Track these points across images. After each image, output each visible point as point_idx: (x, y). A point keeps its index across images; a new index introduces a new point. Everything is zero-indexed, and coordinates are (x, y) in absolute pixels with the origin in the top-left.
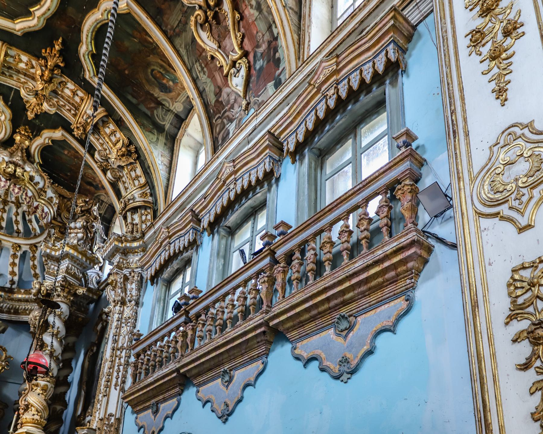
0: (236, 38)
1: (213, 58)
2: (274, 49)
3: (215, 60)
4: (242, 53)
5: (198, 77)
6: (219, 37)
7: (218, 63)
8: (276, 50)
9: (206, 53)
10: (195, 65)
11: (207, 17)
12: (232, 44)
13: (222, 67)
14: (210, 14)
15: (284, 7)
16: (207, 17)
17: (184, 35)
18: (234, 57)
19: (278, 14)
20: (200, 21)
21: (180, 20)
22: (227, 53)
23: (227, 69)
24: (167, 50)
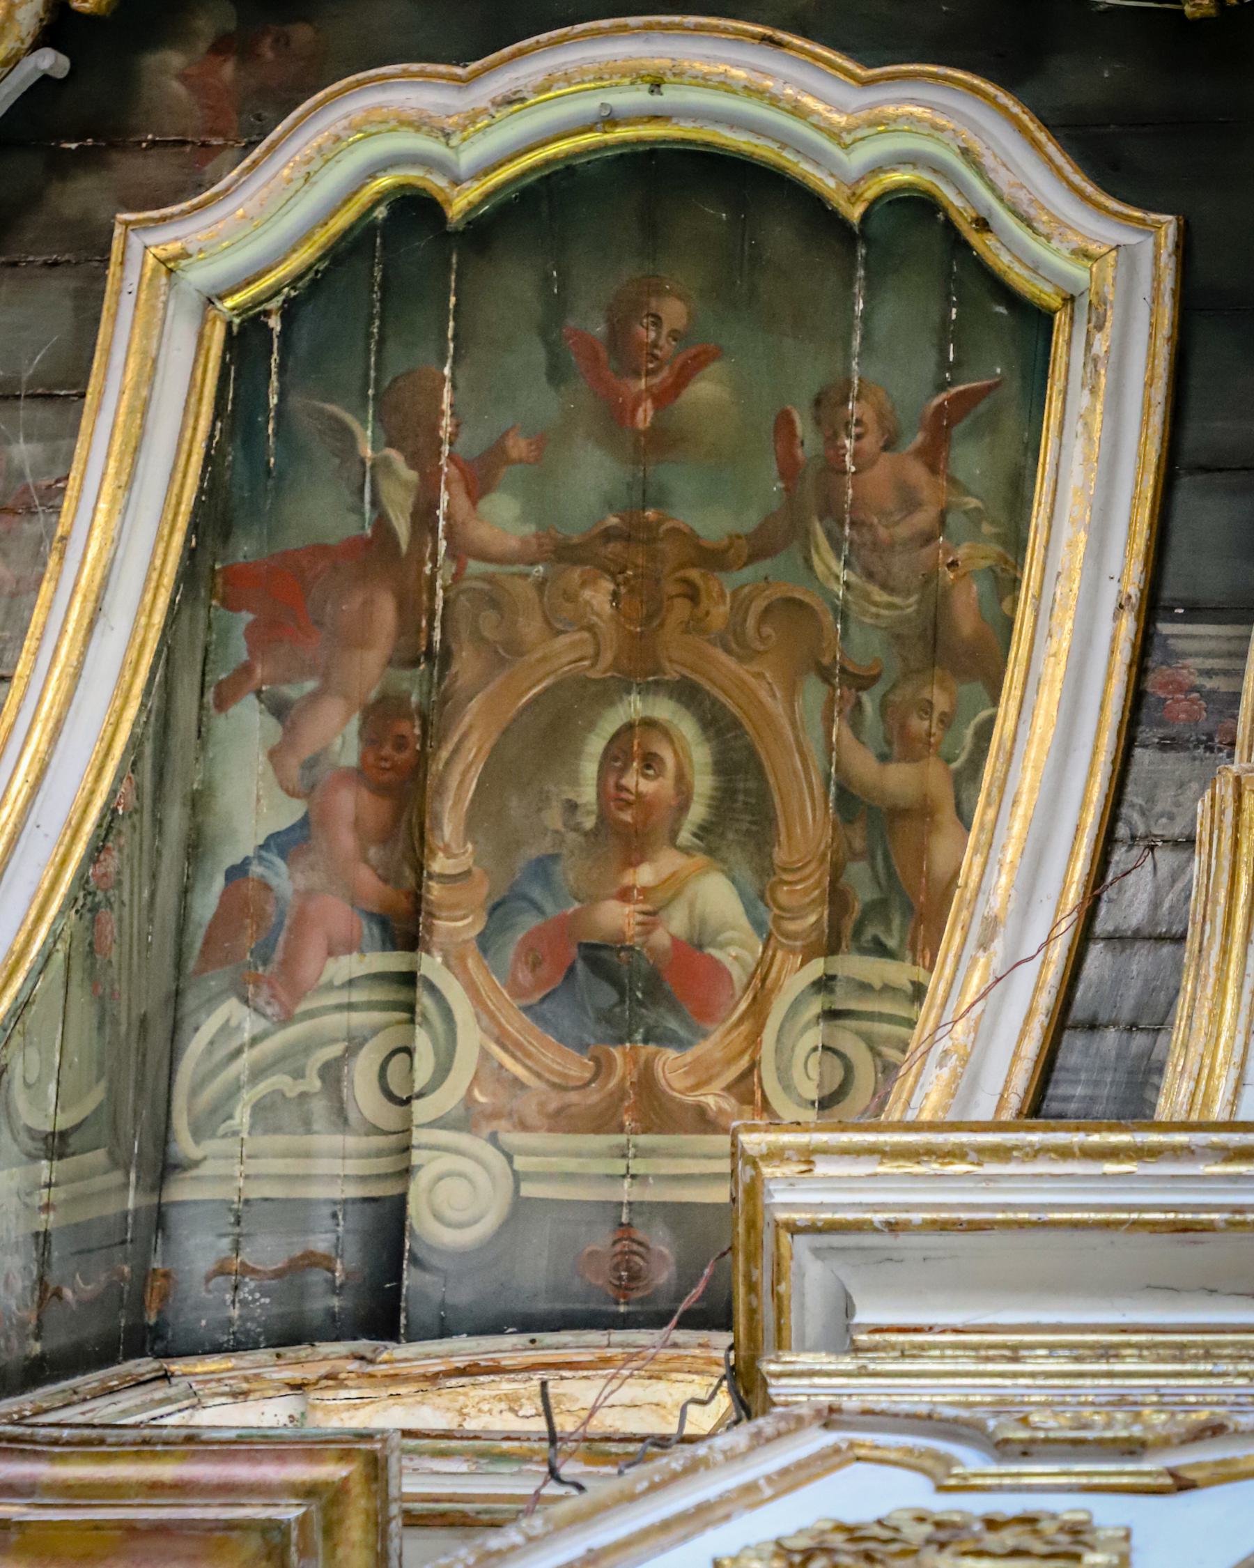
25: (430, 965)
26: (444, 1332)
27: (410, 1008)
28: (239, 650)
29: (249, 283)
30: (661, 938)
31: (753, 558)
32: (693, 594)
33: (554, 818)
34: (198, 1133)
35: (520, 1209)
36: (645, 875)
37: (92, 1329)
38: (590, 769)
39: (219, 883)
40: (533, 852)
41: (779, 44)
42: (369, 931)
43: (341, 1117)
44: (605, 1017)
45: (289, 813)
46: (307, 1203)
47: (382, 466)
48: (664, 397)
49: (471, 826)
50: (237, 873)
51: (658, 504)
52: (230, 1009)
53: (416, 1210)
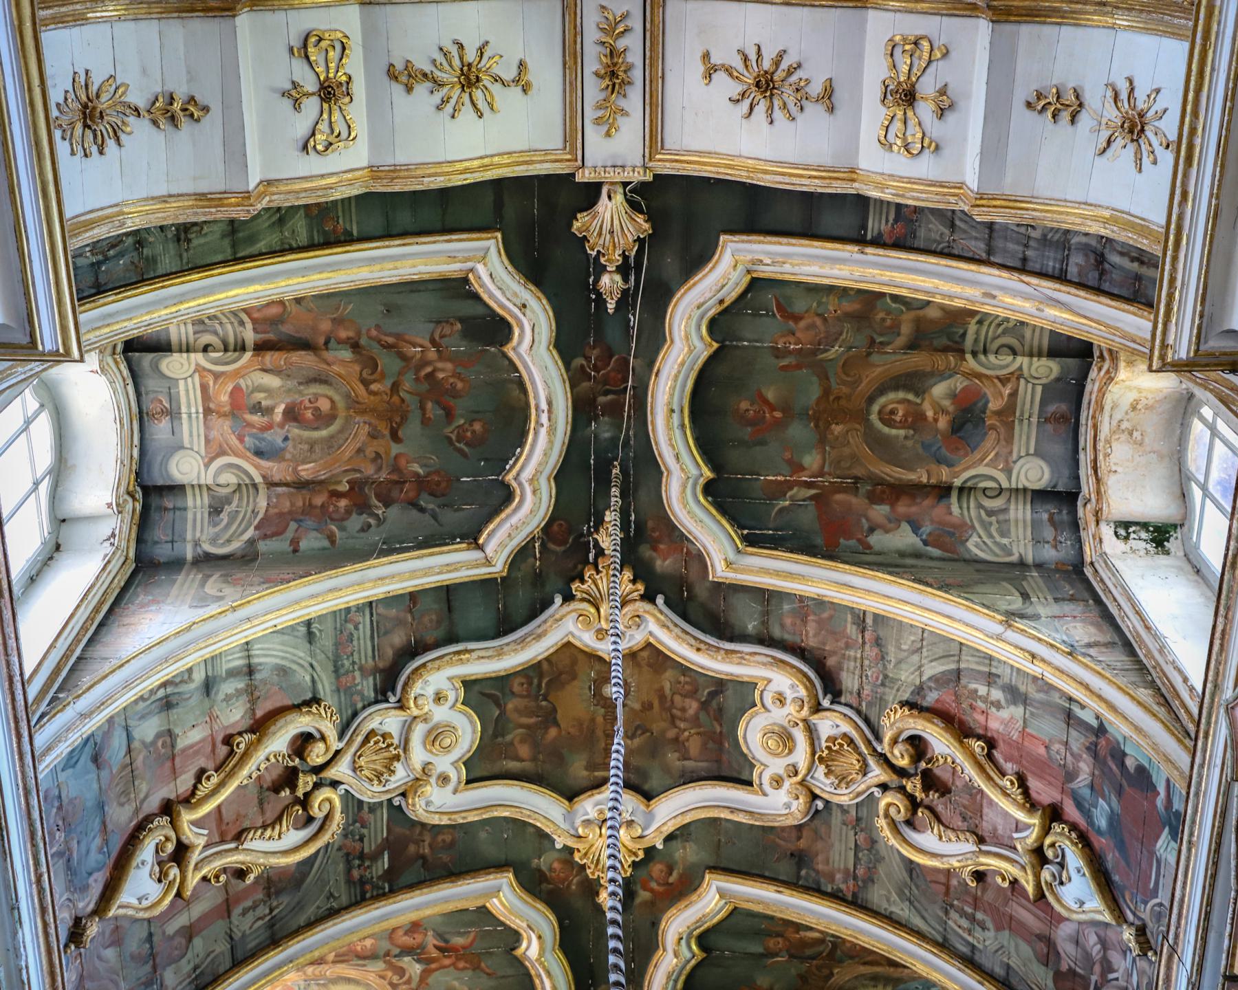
0: (1006, 795)
1: (979, 876)
2: (1113, 756)
3: (989, 879)
4: (1043, 817)
5: (973, 946)
6: (964, 819)
7: (999, 880)
8: (1119, 756)
9: (957, 876)
11: (911, 798)
12: (1006, 814)
13: (1014, 882)
14: (914, 786)
15: (1070, 654)
16: (911, 798)
17: (881, 870)
18: (1030, 841)
19: (1064, 677)
20: (900, 818)
22: (1006, 841)
23: (1031, 878)
24: (862, 931)
25: (958, 482)
26: (1077, 478)
27: (970, 489)
28: (852, 542)
30: (951, 409)
31: (828, 379)
32: (838, 398)
33: (909, 443)
34: (1011, 554)
35: (1037, 454)
36: (930, 414)
37: (1080, 586)
38: (894, 432)
39: (929, 548)
40: (920, 451)
41: (658, 371)
42: (944, 503)
43: (1005, 510)
44: (976, 426)
45: (905, 527)
46: (1033, 521)
47: (792, 498)
48: (773, 408)
49: (911, 469)
50: (926, 543)
51: (807, 410)
52: (970, 545)
53: (1037, 486)
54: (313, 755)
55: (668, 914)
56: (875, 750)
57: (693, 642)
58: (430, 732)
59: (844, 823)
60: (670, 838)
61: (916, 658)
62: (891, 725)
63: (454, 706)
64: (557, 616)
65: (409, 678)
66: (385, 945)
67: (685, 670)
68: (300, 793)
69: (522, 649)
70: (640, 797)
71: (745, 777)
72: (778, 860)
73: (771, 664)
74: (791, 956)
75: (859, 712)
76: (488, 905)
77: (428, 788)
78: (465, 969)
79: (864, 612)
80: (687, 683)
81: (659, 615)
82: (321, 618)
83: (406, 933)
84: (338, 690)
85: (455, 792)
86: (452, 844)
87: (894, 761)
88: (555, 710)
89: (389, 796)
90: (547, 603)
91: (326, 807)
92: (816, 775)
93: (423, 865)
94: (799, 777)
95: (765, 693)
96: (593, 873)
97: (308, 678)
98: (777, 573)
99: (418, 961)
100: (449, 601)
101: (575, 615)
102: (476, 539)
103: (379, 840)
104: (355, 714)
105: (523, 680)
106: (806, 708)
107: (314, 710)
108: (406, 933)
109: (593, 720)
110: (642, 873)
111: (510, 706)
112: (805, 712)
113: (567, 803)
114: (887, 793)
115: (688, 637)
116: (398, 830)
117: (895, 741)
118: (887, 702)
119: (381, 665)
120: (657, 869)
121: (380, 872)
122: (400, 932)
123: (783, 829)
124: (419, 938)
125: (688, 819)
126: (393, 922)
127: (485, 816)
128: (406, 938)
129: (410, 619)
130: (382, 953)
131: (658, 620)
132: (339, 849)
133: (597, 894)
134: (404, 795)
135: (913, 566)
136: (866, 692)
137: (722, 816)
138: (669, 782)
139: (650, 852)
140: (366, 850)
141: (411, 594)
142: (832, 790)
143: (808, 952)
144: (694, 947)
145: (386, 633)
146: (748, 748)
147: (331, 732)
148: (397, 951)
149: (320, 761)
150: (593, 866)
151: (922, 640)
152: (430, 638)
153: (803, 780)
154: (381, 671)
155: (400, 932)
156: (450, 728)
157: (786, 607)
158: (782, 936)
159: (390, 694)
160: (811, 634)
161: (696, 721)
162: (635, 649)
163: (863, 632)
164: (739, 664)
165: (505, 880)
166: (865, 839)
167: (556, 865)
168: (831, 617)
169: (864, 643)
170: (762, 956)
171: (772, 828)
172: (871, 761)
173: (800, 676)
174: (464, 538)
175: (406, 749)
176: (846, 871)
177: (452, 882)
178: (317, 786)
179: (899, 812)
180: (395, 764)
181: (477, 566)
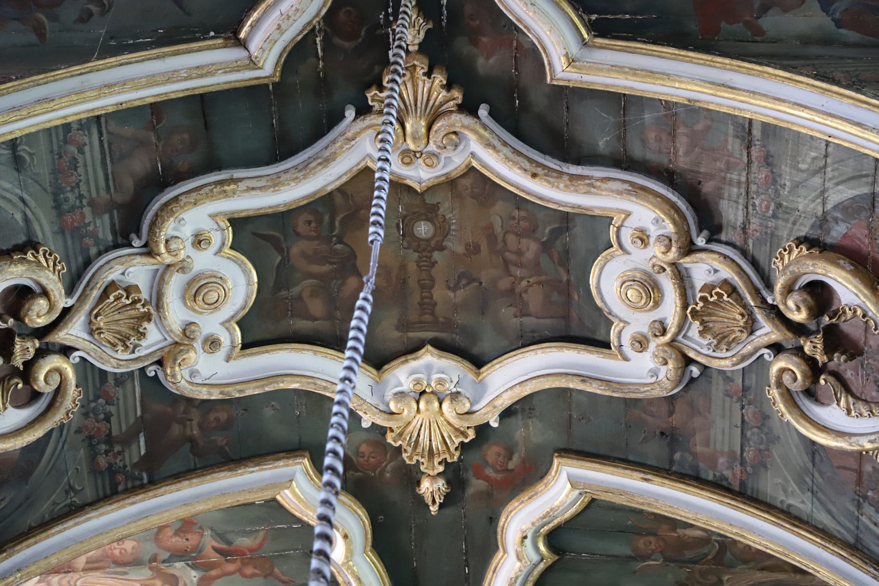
10: (864, 519)
16: (810, 362)
17: (776, 452)
21: (743, 421)
24: (752, 530)
29: (577, 28)
54: (33, 314)
55: (509, 507)
56: (764, 301)
57: (527, 165)
58: (189, 284)
59: (727, 394)
60: (507, 414)
61: (817, 181)
62: (786, 268)
63: (219, 251)
64: (349, 134)
65: (156, 215)
66: (150, 548)
67: (519, 202)
68: (18, 361)
69: (305, 177)
70: (468, 364)
71: (600, 337)
72: (645, 440)
73: (628, 192)
74: (667, 560)
75: (744, 253)
76: (278, 498)
77: (192, 354)
78: (254, 575)
79: (751, 121)
80: (524, 218)
81: (482, 131)
82: (30, 138)
83: (176, 533)
84: (62, 231)
85: (228, 359)
86: (226, 426)
87: (790, 316)
88: (353, 255)
89: (141, 365)
90: (337, 117)
91: (56, 379)
92: (690, 334)
93: (192, 448)
94: (668, 337)
95: (623, 230)
96: (410, 458)
97: (18, 217)
98: (634, 71)
99: (194, 567)
100: (204, 115)
101: (371, 132)
102: (236, 33)
103: (132, 420)
104: (88, 263)
105: (311, 218)
106: (674, 249)
107: (29, 256)
108: (176, 533)
109: (403, 267)
110: (474, 457)
111: (295, 250)
112: (673, 254)
113: (374, 371)
114: (780, 356)
115: (520, 159)
116: (158, 407)
117: (789, 290)
118: (780, 239)
119: (119, 199)
120: (492, 452)
121: (136, 459)
122: (169, 532)
123: (651, 401)
124: (193, 539)
125: (528, 390)
126: (156, 520)
127: (267, 389)
128: (175, 539)
129: (153, 139)
130: (147, 558)
131: (481, 137)
132: (78, 431)
133: (418, 483)
134: (160, 363)
135: (818, 57)
136: (752, 226)
137: (571, 386)
138: (505, 343)
139: (483, 430)
140: (115, 432)
141: (152, 105)
142: (710, 352)
143: (689, 554)
144: (542, 548)
145: (123, 157)
146: (602, 299)
147: (56, 288)
148: (166, 555)
149: (42, 322)
150: (410, 449)
151: (826, 156)
152: (183, 162)
153: (673, 340)
154: (120, 207)
155: (169, 532)
156: (217, 280)
157: (648, 117)
158: (655, 534)
159: (133, 236)
160: (681, 153)
161: (536, 267)
162: (454, 175)
163: (748, 148)
164: (588, 193)
165: (299, 467)
166: (754, 414)
167: (364, 448)
168: (708, 128)
169: (750, 162)
170: (630, 558)
171: (637, 401)
172: (759, 315)
173: (666, 207)
174: (219, 31)
175: (159, 306)
176: (732, 453)
177: (231, 470)
178: (41, 353)
179: (795, 379)
180: (145, 324)
181: (237, 69)
